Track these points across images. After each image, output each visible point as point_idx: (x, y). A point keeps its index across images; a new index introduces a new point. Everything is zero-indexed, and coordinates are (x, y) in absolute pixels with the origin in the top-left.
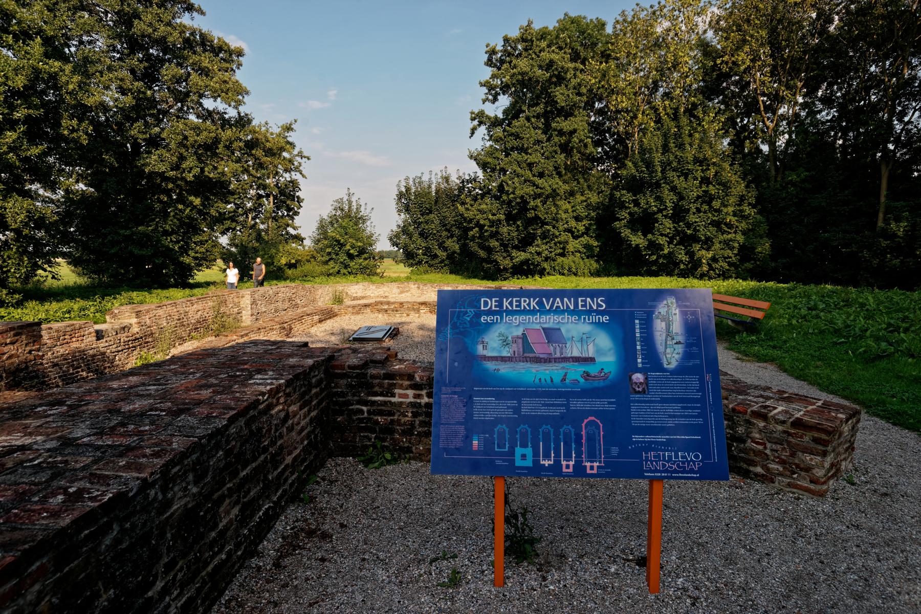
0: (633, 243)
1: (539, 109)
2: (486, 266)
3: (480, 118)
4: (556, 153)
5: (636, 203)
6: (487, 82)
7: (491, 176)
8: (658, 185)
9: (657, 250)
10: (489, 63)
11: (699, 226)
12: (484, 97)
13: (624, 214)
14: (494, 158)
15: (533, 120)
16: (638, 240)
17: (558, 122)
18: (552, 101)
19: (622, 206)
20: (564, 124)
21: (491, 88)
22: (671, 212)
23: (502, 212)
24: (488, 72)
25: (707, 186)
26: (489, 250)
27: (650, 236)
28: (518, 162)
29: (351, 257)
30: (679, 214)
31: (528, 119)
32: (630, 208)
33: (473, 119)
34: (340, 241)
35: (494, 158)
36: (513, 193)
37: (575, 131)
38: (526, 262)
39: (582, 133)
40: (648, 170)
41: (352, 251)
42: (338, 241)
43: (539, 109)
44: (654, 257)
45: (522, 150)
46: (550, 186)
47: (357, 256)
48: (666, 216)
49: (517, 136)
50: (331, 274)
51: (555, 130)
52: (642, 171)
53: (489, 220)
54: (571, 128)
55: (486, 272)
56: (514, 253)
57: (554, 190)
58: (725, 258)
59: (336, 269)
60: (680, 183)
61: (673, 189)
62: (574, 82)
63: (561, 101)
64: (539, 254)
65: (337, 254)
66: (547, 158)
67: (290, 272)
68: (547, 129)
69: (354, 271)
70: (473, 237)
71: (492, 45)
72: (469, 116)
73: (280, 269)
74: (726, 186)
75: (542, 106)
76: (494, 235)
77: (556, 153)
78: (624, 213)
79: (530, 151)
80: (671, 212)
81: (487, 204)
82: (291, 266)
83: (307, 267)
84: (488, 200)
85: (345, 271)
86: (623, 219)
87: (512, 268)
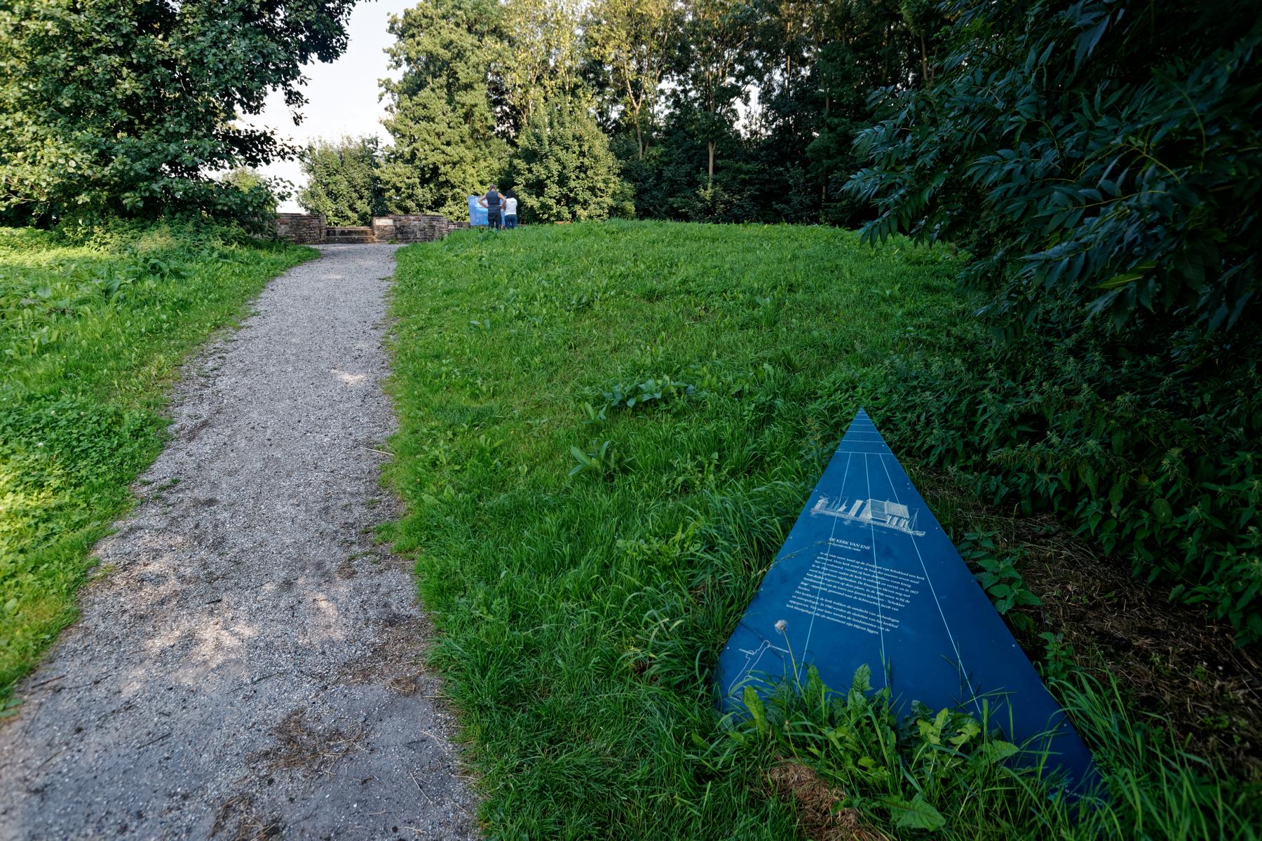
3: (387, 85)
5: (530, 171)
13: (520, 180)
18: (453, 74)
19: (519, 173)
23: (416, 175)
27: (541, 198)
30: (562, 181)
31: (433, 90)
36: (426, 159)
43: (443, 80)
45: (430, 119)
48: (553, 182)
49: (425, 107)
51: (458, 103)
54: (473, 103)
57: (461, 158)
60: (562, 155)
61: (558, 160)
74: (596, 158)
75: (445, 78)
76: (410, 196)
81: (401, 168)
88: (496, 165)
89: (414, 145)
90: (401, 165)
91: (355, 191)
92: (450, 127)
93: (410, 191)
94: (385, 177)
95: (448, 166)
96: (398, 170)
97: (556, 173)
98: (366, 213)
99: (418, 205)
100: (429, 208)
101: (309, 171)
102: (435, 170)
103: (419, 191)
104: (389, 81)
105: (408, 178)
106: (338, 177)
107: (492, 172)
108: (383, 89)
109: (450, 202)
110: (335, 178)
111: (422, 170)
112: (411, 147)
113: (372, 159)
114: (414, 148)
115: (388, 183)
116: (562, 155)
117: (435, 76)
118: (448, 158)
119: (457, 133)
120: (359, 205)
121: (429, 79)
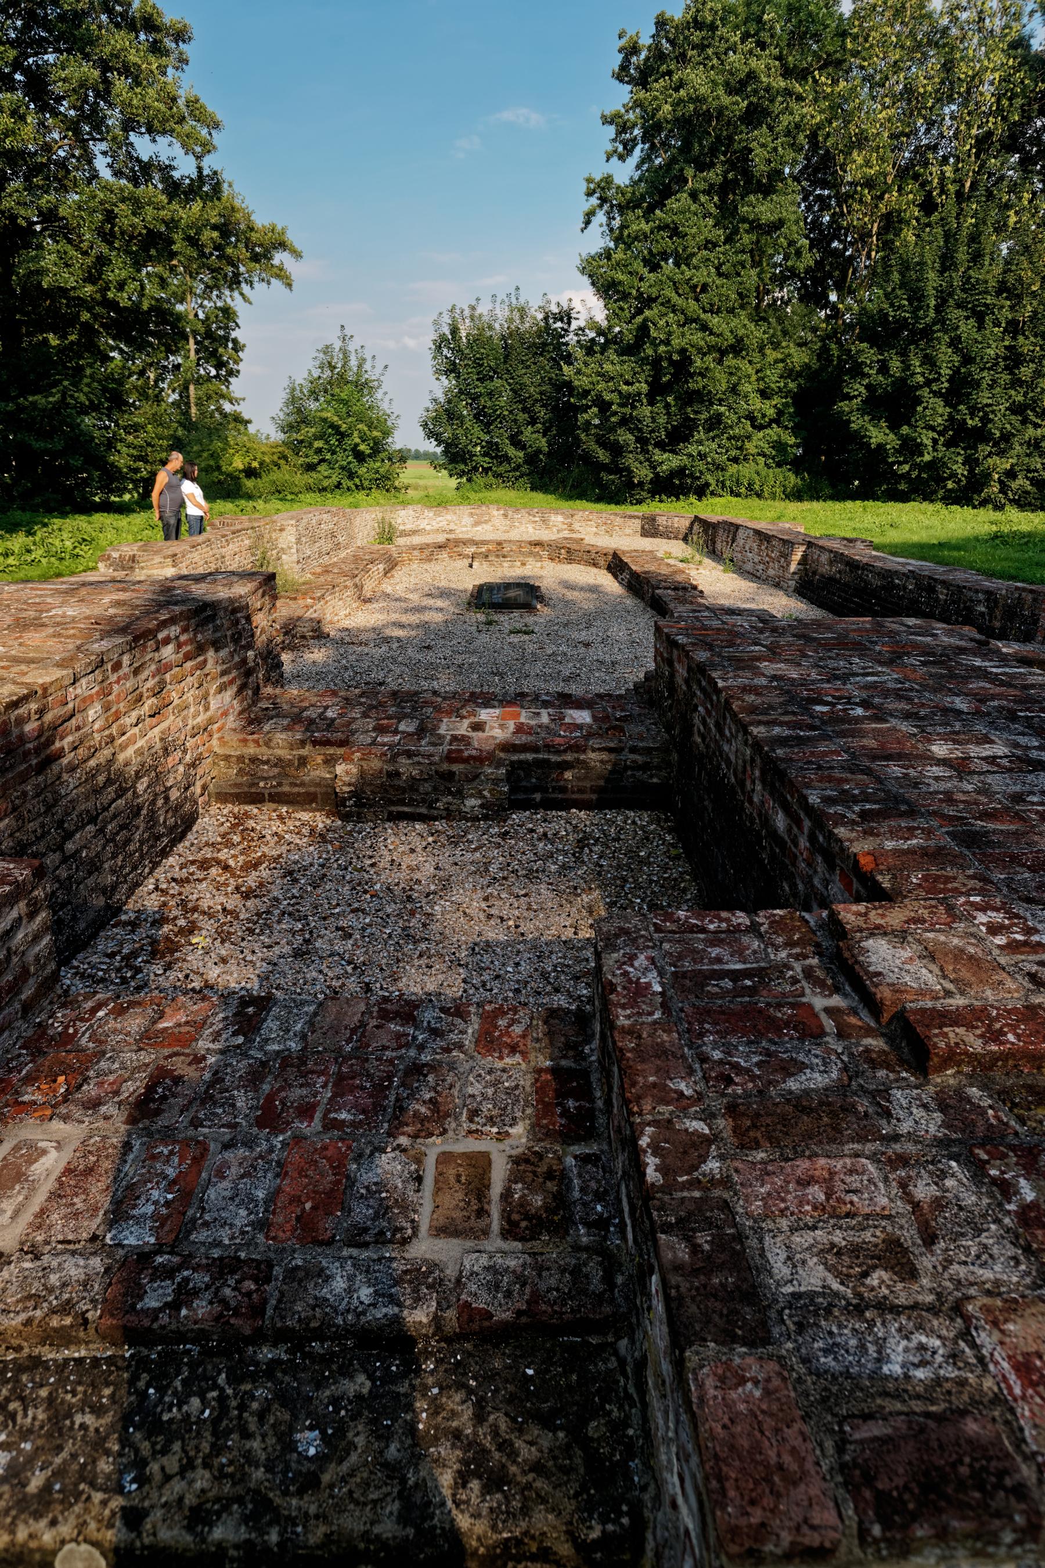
0: (873, 440)
1: (714, 175)
2: (605, 477)
4: (744, 267)
6: (618, 115)
7: (622, 309)
8: (927, 333)
9: (913, 454)
10: (622, 74)
11: (993, 412)
12: (610, 147)
13: (858, 388)
14: (630, 273)
15: (703, 198)
16: (878, 435)
17: (750, 205)
18: (741, 160)
19: (857, 371)
20: (763, 208)
21: (623, 128)
22: (946, 385)
23: (642, 377)
24: (621, 96)
25: (1014, 338)
26: (617, 450)
27: (905, 430)
28: (675, 283)
29: (360, 457)
31: (694, 195)
32: (869, 376)
33: (590, 194)
34: (339, 427)
35: (630, 273)
37: (780, 223)
38: (681, 472)
39: (794, 228)
40: (911, 304)
41: (362, 447)
42: (336, 428)
44: (906, 468)
46: (731, 332)
47: (370, 456)
48: (936, 394)
50: (324, 489)
51: (744, 220)
52: (900, 307)
53: (620, 393)
54: (773, 217)
55: (603, 487)
56: (658, 456)
57: (740, 340)
58: (1029, 471)
59: (335, 479)
62: (785, 120)
63: (759, 162)
64: (702, 456)
65: (334, 453)
66: (727, 276)
67: (249, 484)
68: (727, 214)
69: (366, 483)
70: (588, 423)
71: (631, 32)
72: (583, 187)
73: (233, 477)
76: (624, 421)
77: (744, 267)
78: (857, 386)
79: (694, 261)
80: (946, 385)
81: (613, 364)
82: (250, 473)
83: (276, 475)
84: (612, 355)
85: (350, 484)
86: (855, 397)
87: (651, 482)
88: (799, 357)
89: (647, 313)
90: (614, 357)
91: (524, 410)
92: (720, 275)
93: (627, 410)
94: (582, 382)
95: (709, 358)
96: (607, 367)
97: (946, 372)
98: (539, 451)
99: (638, 440)
100: (661, 445)
101: (447, 373)
102: (682, 365)
103: (646, 411)
104: (608, 180)
105: (627, 383)
106: (497, 382)
107: (789, 374)
108: (594, 201)
109: (700, 434)
110: (491, 385)
111: (656, 363)
112: (639, 319)
113: (558, 346)
114: (646, 320)
115: (586, 393)
116: (967, 328)
117: (701, 167)
118: (712, 340)
119: (734, 287)
120: (528, 434)
121: (689, 172)
